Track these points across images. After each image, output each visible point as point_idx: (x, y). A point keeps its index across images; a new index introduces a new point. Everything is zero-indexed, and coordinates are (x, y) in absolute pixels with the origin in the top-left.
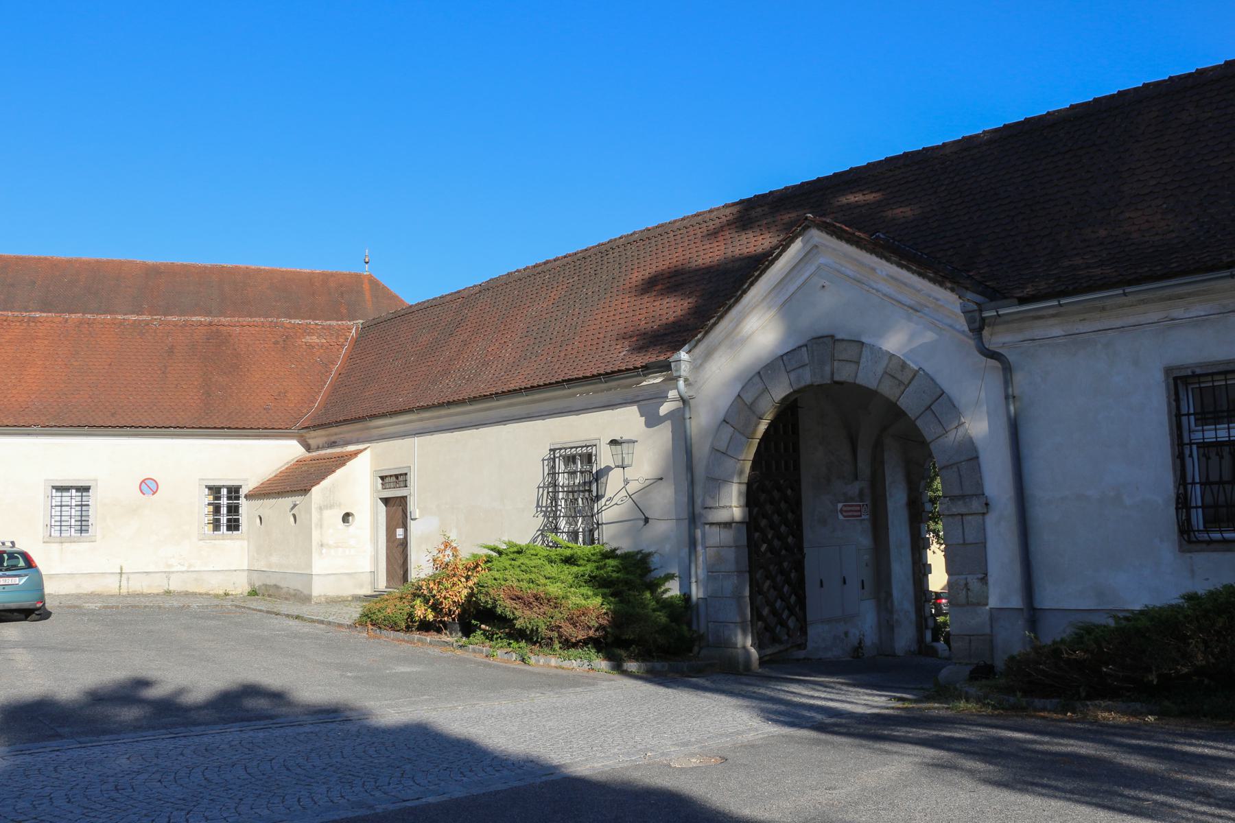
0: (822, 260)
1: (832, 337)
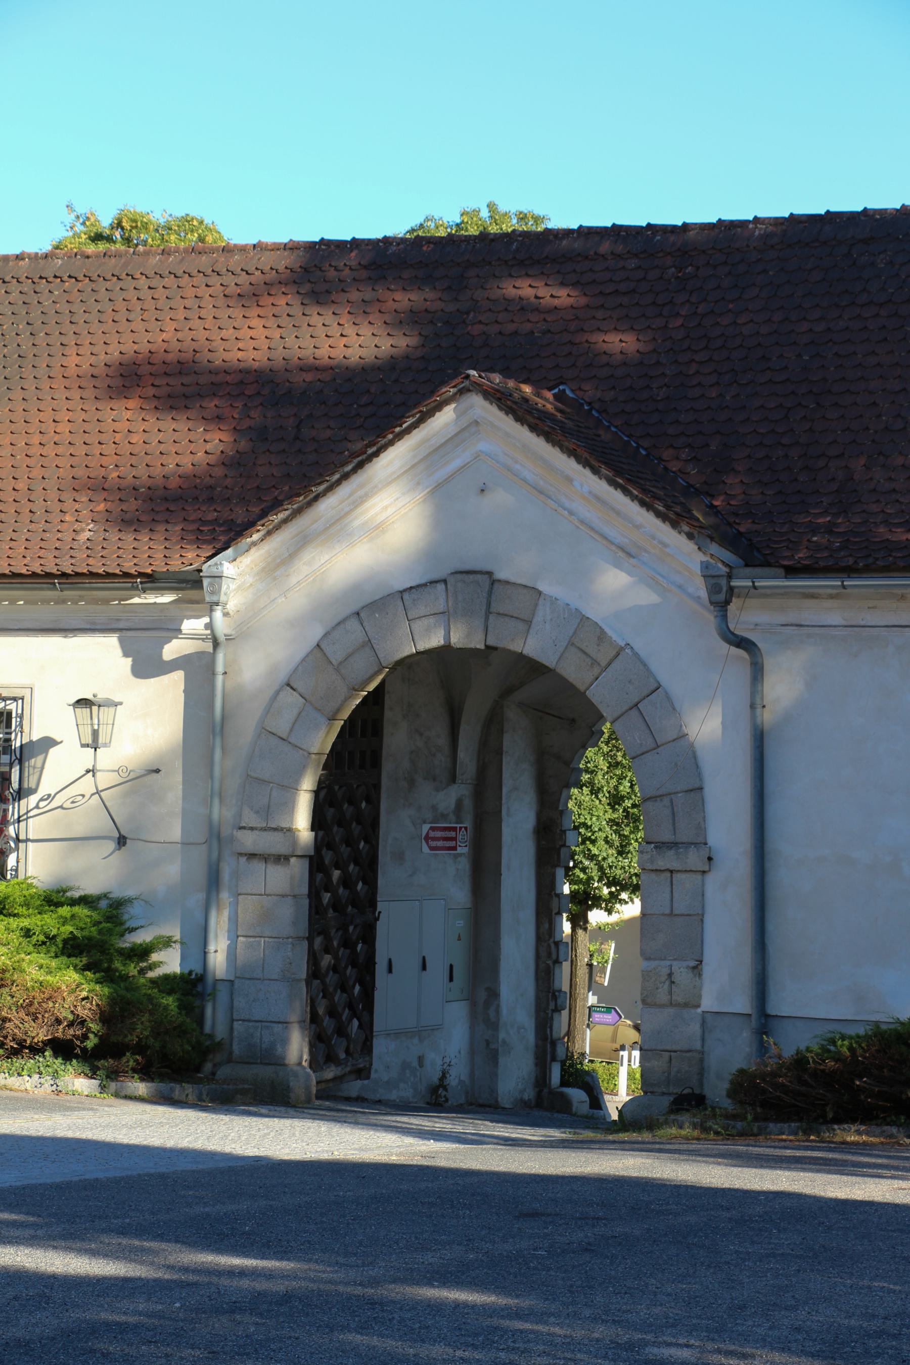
0: (483, 446)
1: (490, 574)
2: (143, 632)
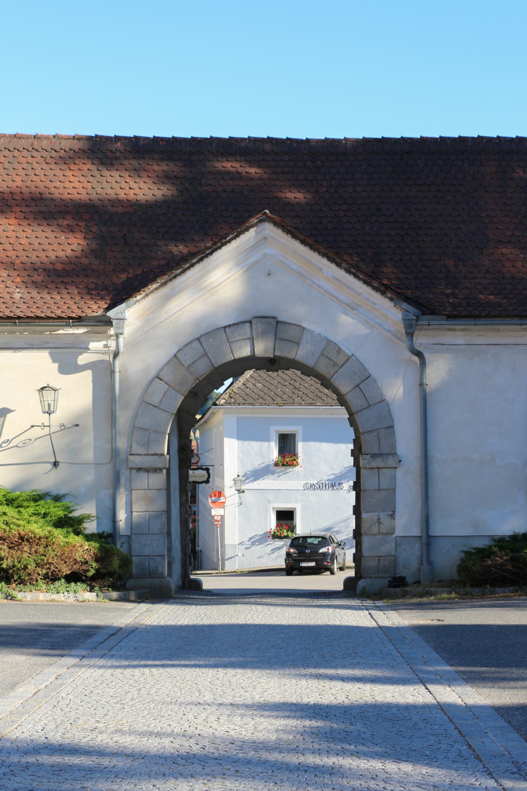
0: (267, 250)
2: (65, 349)
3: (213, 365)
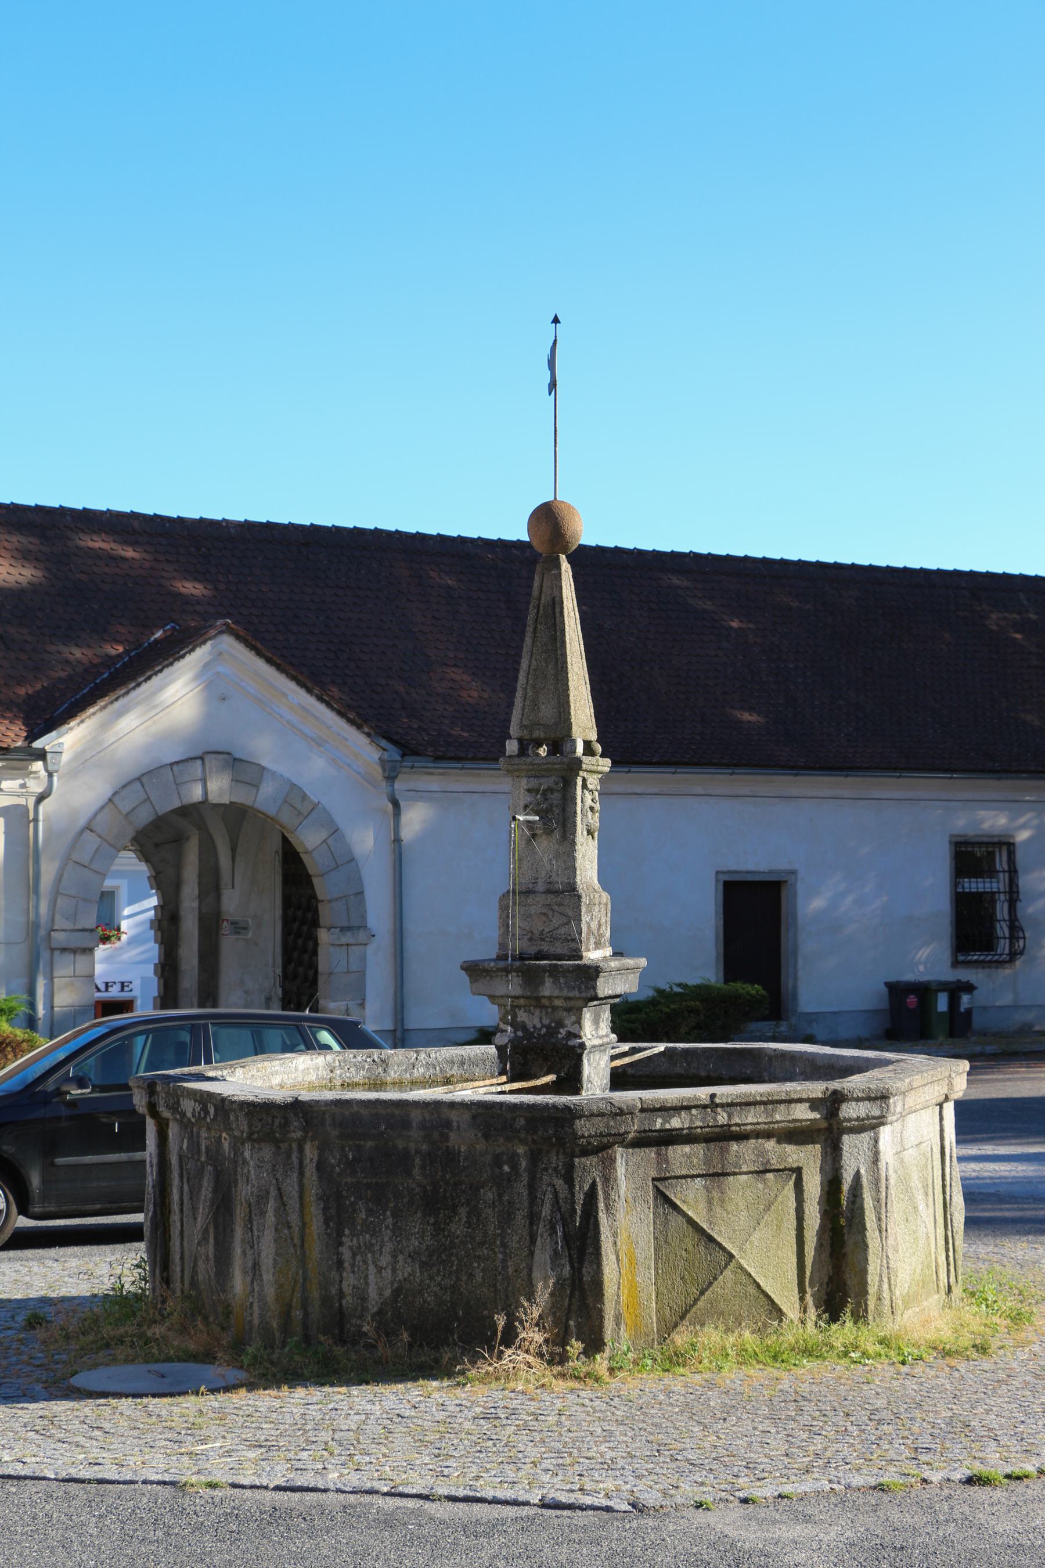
0: (220, 669)
3: (156, 813)
